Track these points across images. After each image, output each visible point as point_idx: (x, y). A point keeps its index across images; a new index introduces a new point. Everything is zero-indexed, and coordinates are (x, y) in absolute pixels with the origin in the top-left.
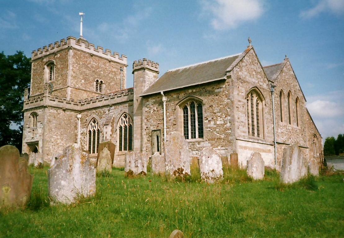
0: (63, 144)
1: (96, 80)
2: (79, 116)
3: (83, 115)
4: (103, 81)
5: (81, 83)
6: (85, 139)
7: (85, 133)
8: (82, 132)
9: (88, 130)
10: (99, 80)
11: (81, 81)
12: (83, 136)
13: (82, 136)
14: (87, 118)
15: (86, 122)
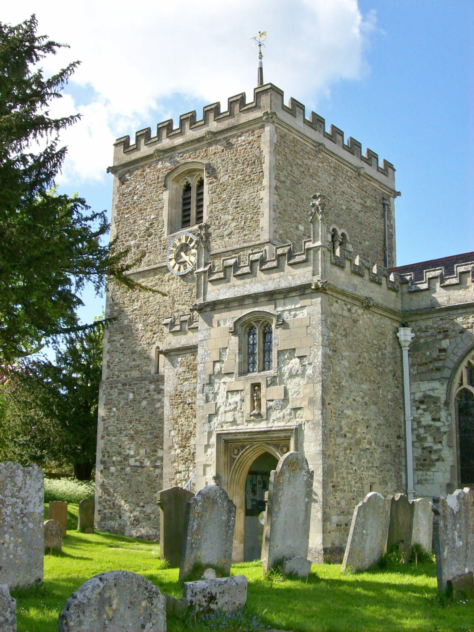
0: (370, 443)
1: (331, 229)
2: (406, 335)
3: (420, 330)
4: (346, 233)
5: (298, 232)
6: (438, 424)
7: (438, 398)
8: (419, 396)
9: (455, 390)
10: (338, 229)
11: (297, 228)
12: (424, 410)
13: (420, 411)
14: (445, 343)
15: (438, 359)
